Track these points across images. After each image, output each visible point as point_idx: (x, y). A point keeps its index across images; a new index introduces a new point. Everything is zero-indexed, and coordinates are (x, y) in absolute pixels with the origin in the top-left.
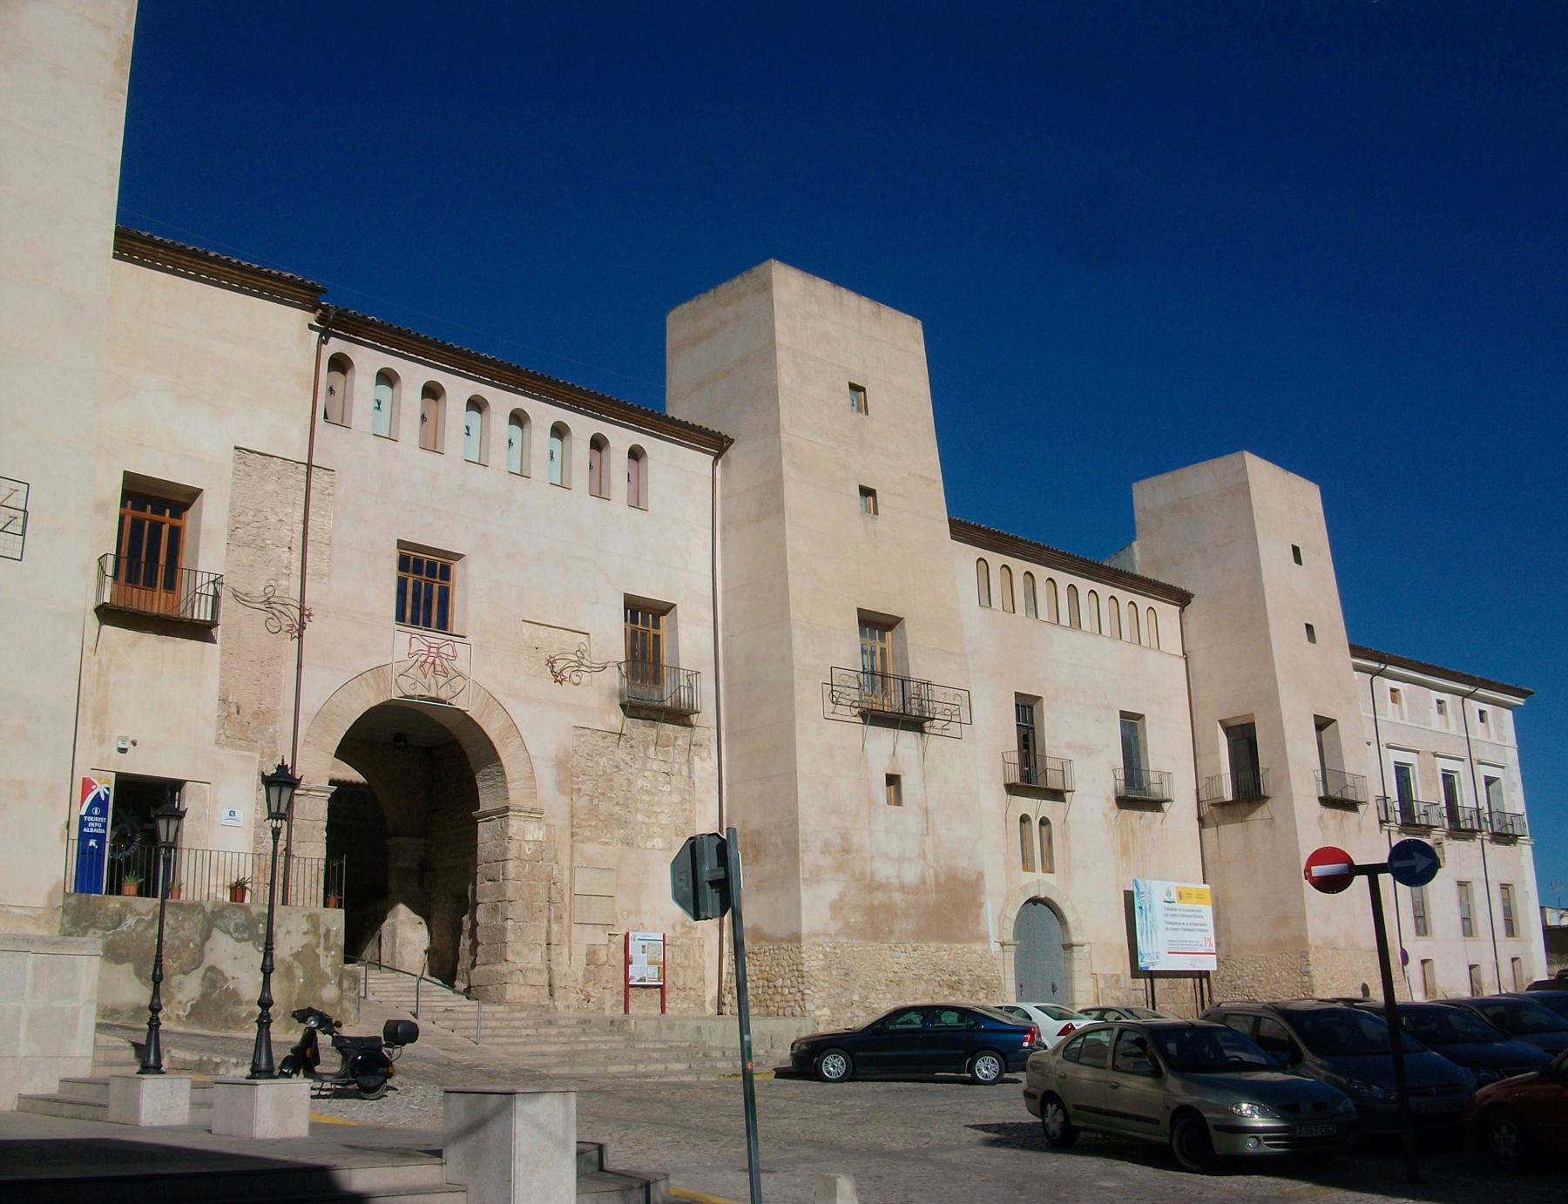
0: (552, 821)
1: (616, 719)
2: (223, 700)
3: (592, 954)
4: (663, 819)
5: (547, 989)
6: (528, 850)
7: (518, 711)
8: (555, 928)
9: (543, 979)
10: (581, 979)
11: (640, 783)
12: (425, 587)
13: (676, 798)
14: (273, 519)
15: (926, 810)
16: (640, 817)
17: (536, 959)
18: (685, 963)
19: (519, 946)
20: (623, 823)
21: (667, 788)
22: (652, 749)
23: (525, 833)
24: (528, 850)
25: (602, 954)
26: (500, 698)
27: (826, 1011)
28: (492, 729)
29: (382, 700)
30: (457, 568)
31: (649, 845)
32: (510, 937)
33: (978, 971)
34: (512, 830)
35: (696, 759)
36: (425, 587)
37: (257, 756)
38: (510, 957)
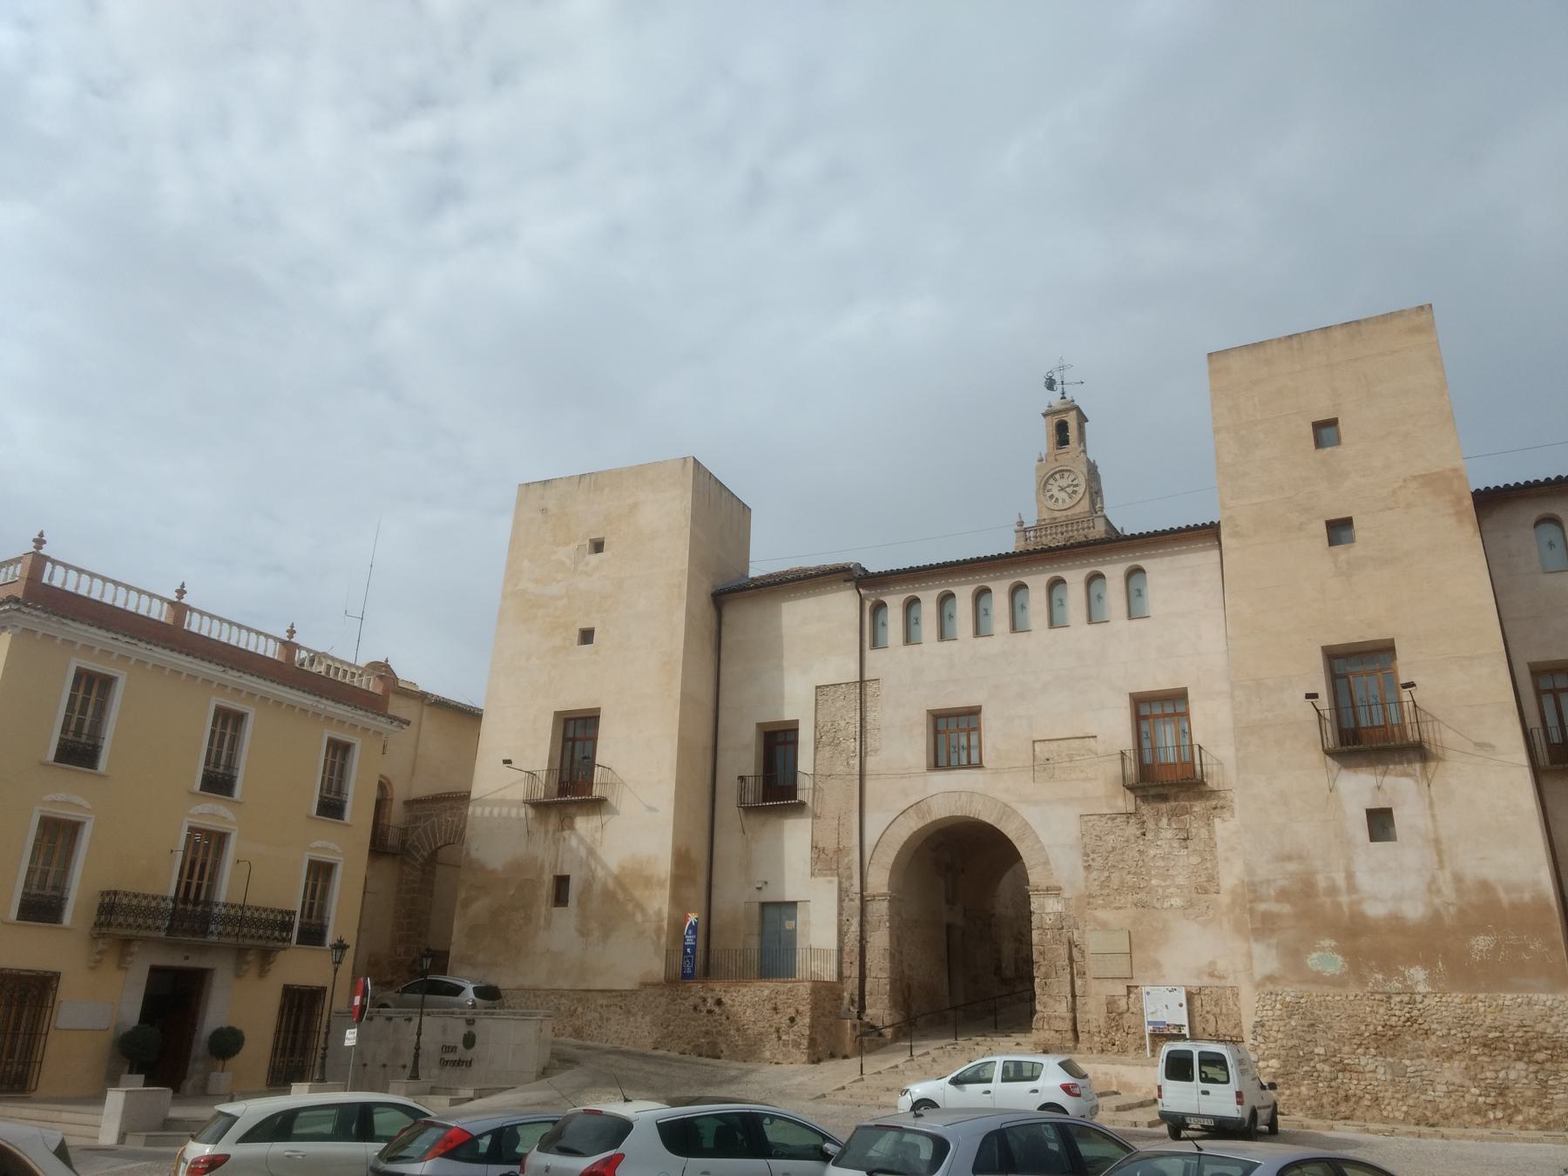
0: (1067, 895)
1: (1125, 802)
2: (814, 847)
3: (1111, 1003)
4: (1180, 880)
5: (1070, 1035)
6: (1049, 921)
7: (1030, 814)
8: (1078, 982)
9: (1067, 1025)
10: (1102, 1022)
11: (1152, 852)
12: (952, 734)
13: (1195, 860)
14: (843, 723)
15: (1437, 842)
16: (1154, 882)
17: (1063, 1009)
18: (1217, 1010)
19: (1045, 998)
20: (1136, 889)
21: (1185, 852)
22: (1164, 821)
23: (1045, 909)
24: (1049, 921)
25: (1123, 1004)
26: (1014, 805)
27: (1274, 1063)
28: (1009, 830)
29: (920, 825)
30: (984, 715)
31: (1166, 905)
32: (1038, 991)
33: (1539, 1027)
34: (1034, 907)
35: (1217, 821)
36: (952, 734)
37: (836, 879)
38: (1038, 1007)
